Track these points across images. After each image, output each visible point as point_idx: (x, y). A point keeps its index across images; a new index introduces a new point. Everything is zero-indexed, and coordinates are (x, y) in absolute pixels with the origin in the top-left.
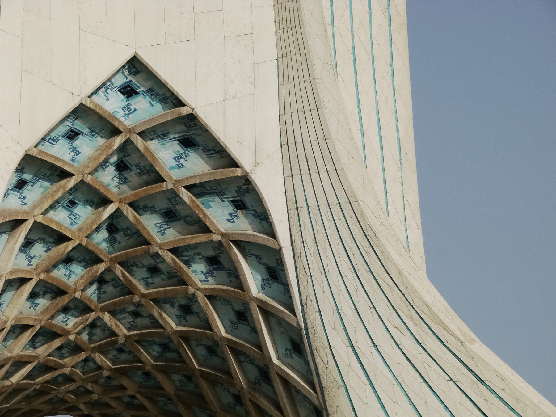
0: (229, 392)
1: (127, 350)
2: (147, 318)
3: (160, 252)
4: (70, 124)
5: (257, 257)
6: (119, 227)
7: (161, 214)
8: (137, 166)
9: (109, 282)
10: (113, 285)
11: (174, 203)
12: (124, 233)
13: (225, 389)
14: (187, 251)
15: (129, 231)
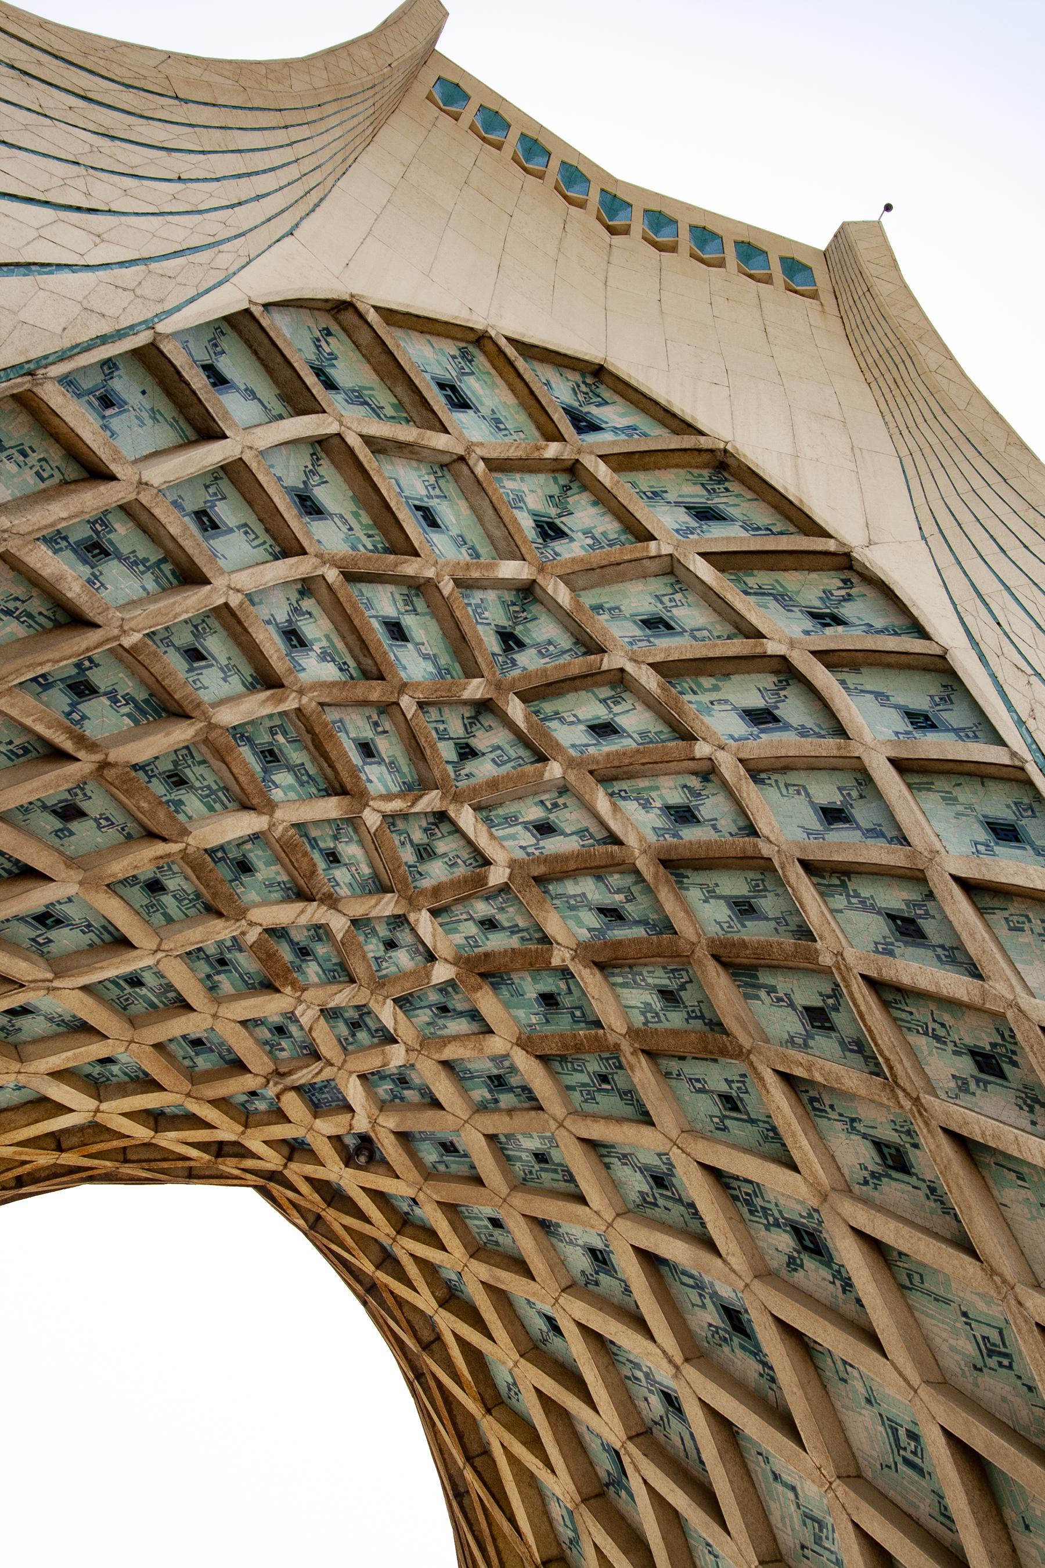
0: (792, 1005)
1: (506, 924)
2: (575, 837)
3: (630, 667)
4: (454, 374)
5: (877, 695)
6: (526, 640)
7: (635, 622)
8: (587, 532)
9: (483, 754)
10: (493, 760)
11: (669, 604)
12: (540, 652)
13: (780, 1000)
14: (695, 693)
15: (551, 648)
